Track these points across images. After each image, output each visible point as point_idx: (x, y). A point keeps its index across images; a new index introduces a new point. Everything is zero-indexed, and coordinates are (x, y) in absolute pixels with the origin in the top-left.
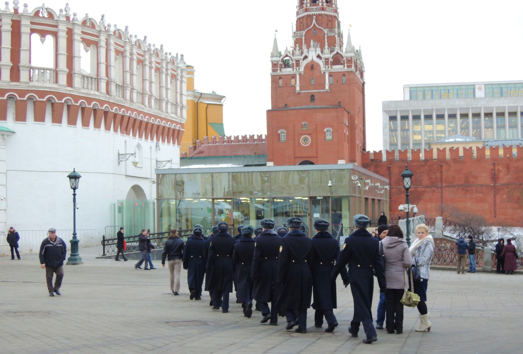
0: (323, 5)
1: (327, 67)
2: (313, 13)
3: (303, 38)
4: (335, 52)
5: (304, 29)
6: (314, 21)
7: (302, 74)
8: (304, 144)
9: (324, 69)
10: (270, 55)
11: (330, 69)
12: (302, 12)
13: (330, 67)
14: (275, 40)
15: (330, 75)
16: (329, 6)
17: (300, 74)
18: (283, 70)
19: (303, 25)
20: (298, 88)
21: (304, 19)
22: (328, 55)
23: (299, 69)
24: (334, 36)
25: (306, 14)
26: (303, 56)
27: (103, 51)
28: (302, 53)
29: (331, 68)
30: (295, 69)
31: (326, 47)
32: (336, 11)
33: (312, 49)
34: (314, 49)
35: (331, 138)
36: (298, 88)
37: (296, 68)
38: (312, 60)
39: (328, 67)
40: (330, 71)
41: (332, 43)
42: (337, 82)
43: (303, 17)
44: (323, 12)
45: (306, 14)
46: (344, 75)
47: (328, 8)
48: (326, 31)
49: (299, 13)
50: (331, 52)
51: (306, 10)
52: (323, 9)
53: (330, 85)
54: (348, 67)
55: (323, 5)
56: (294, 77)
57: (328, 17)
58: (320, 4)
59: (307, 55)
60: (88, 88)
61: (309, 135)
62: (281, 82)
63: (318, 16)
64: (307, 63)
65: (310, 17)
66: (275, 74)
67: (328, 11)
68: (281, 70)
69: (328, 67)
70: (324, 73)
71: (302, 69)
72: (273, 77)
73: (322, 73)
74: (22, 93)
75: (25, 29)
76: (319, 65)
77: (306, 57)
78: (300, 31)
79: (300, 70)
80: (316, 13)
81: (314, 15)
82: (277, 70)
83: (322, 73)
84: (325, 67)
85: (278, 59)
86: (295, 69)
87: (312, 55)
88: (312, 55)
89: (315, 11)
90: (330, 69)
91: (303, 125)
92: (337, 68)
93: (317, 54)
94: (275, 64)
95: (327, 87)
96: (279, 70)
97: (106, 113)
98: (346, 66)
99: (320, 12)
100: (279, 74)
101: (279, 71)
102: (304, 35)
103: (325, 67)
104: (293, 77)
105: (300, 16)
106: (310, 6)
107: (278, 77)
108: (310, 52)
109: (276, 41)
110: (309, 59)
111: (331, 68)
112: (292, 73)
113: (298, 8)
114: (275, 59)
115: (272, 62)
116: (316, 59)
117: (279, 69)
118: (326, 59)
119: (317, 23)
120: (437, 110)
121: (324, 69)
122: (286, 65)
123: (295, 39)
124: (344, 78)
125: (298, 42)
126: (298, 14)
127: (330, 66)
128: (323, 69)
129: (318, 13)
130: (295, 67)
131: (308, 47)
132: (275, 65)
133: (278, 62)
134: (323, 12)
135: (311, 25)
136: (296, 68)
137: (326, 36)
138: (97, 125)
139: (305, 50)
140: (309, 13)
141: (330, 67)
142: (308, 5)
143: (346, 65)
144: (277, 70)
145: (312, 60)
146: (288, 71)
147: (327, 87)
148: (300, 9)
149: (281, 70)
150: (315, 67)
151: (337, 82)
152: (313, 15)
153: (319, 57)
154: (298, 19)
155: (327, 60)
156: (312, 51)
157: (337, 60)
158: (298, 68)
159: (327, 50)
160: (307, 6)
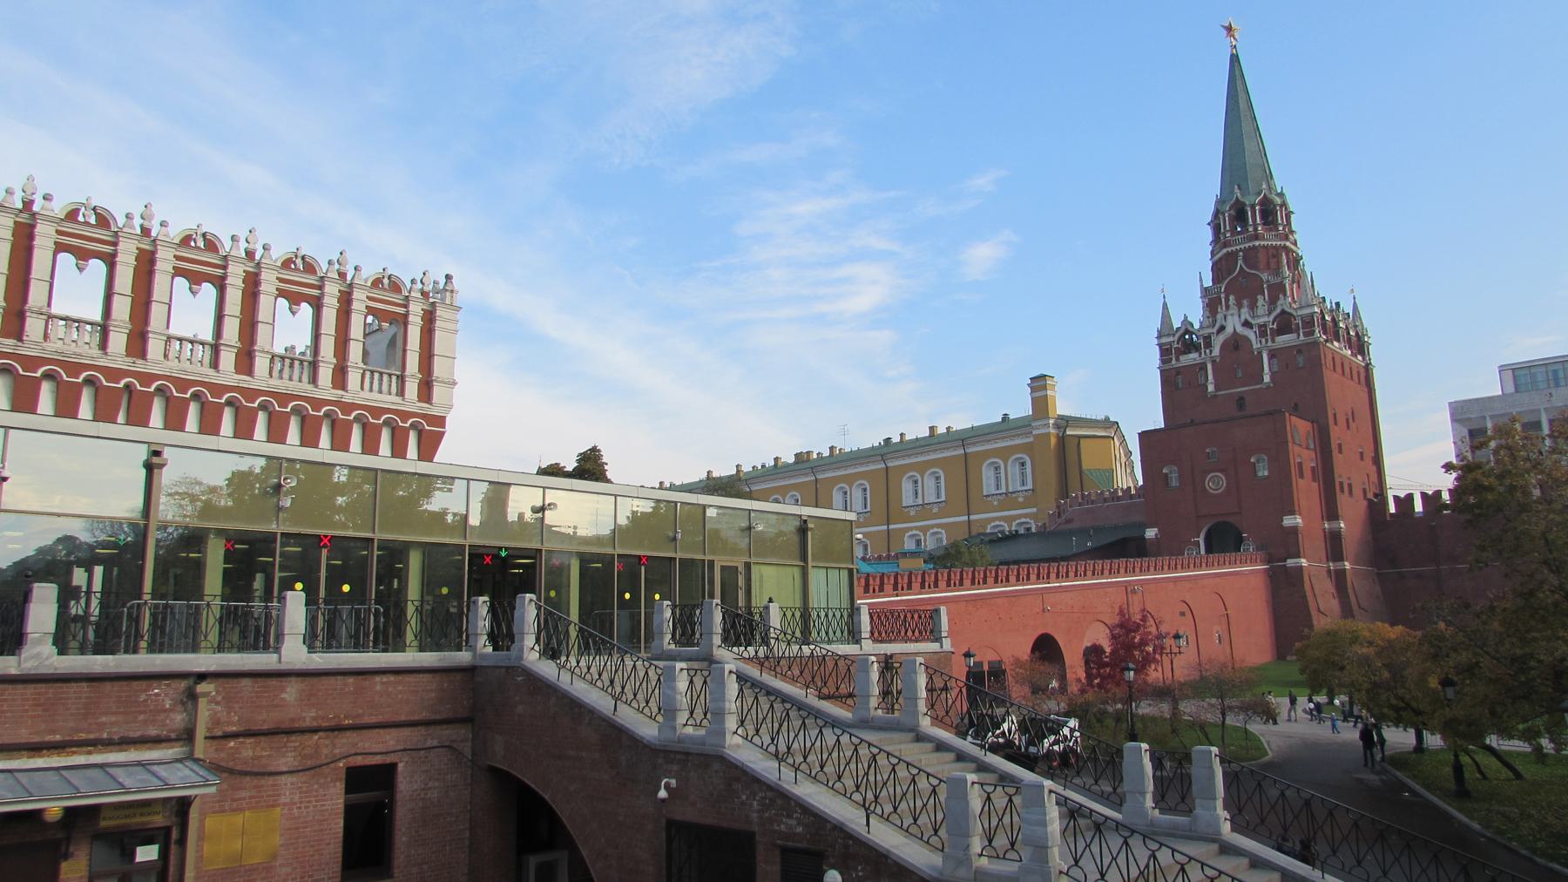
1: (1263, 340)
2: (1238, 248)
4: (1278, 311)
6: (1240, 262)
7: (1218, 360)
8: (1214, 490)
9: (1259, 345)
11: (1270, 344)
14: (1165, 306)
15: (1272, 356)
16: (1271, 230)
17: (1214, 362)
18: (1182, 358)
20: (1211, 388)
21: (1223, 262)
22: (1264, 317)
23: (1211, 352)
25: (1225, 251)
28: (1215, 322)
29: (1273, 341)
35: (1266, 473)
36: (1211, 388)
39: (1267, 341)
40: (1271, 348)
42: (1287, 368)
44: (1257, 243)
45: (1225, 251)
46: (1299, 352)
48: (1264, 276)
51: (1225, 245)
52: (1256, 237)
53: (1273, 375)
54: (1306, 334)
55: (1256, 229)
58: (1251, 229)
59: (1225, 324)
61: (1221, 471)
66: (1167, 367)
67: (1267, 240)
68: (1177, 360)
69: (1267, 341)
70: (1260, 353)
71: (1216, 352)
76: (1248, 340)
78: (1218, 283)
79: (1213, 355)
80: (1242, 247)
81: (1241, 250)
85: (1171, 339)
87: (1233, 324)
89: (1242, 243)
90: (1270, 344)
91: (1209, 453)
95: (1267, 379)
96: (1174, 359)
101: (1174, 362)
102: (1223, 290)
104: (1201, 369)
107: (1174, 373)
108: (1229, 318)
109: (1167, 308)
110: (1229, 330)
111: (1273, 341)
114: (1164, 340)
115: (1160, 345)
116: (1240, 329)
118: (1260, 326)
119: (1246, 266)
121: (1259, 345)
122: (1190, 346)
124: (1300, 360)
126: (1213, 254)
127: (1269, 337)
128: (1256, 346)
129: (1247, 245)
132: (1165, 352)
134: (1257, 243)
135: (1234, 271)
137: (1265, 286)
140: (1229, 249)
142: (1228, 235)
144: (1171, 359)
146: (1192, 358)
147: (1267, 379)
149: (1177, 360)
151: (1287, 368)
153: (1246, 324)
155: (1263, 328)
156: (1232, 315)
157: (1285, 324)
160: (1226, 237)
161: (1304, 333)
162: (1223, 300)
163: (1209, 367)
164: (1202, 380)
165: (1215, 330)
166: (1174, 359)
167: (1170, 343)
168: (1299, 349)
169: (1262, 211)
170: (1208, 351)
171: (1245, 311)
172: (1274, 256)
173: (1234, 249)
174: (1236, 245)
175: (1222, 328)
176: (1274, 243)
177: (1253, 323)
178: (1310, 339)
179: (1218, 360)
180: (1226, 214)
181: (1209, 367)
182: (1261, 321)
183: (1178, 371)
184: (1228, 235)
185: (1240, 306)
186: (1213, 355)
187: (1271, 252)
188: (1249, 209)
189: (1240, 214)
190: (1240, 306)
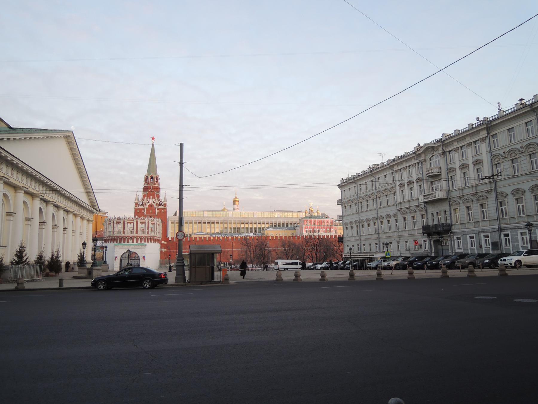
6: (151, 188)
10: (134, 200)
15: (158, 209)
16: (157, 183)
17: (146, 208)
20: (145, 213)
25: (148, 185)
26: (148, 201)
28: (147, 200)
31: (157, 199)
32: (159, 185)
33: (151, 199)
34: (152, 199)
36: (145, 213)
38: (151, 203)
41: (158, 196)
44: (155, 185)
45: (148, 185)
46: (163, 210)
47: (156, 184)
48: (156, 192)
50: (159, 201)
51: (149, 184)
52: (155, 184)
54: (165, 207)
56: (144, 209)
58: (154, 182)
62: (138, 211)
63: (152, 186)
65: (150, 186)
66: (136, 207)
71: (147, 206)
74: (149, 237)
75: (150, 223)
76: (153, 205)
77: (149, 202)
82: (137, 206)
87: (151, 201)
88: (151, 201)
92: (161, 207)
95: (156, 214)
97: (153, 239)
99: (154, 185)
105: (145, 186)
108: (150, 200)
110: (150, 203)
112: (143, 207)
114: (136, 202)
115: (135, 203)
118: (156, 203)
120: (190, 221)
123: (143, 194)
124: (163, 211)
125: (144, 196)
126: (144, 184)
131: (150, 199)
134: (155, 185)
138: (154, 242)
139: (149, 199)
142: (149, 182)
145: (151, 203)
147: (156, 214)
150: (152, 206)
153: (154, 202)
154: (144, 187)
155: (157, 204)
159: (157, 200)
163: (145, 209)
164: (143, 212)
167: (137, 203)
171: (154, 200)
178: (165, 208)
181: (145, 209)
183: (138, 209)
184: (149, 182)
185: (153, 199)
189: (152, 178)
190: (153, 199)
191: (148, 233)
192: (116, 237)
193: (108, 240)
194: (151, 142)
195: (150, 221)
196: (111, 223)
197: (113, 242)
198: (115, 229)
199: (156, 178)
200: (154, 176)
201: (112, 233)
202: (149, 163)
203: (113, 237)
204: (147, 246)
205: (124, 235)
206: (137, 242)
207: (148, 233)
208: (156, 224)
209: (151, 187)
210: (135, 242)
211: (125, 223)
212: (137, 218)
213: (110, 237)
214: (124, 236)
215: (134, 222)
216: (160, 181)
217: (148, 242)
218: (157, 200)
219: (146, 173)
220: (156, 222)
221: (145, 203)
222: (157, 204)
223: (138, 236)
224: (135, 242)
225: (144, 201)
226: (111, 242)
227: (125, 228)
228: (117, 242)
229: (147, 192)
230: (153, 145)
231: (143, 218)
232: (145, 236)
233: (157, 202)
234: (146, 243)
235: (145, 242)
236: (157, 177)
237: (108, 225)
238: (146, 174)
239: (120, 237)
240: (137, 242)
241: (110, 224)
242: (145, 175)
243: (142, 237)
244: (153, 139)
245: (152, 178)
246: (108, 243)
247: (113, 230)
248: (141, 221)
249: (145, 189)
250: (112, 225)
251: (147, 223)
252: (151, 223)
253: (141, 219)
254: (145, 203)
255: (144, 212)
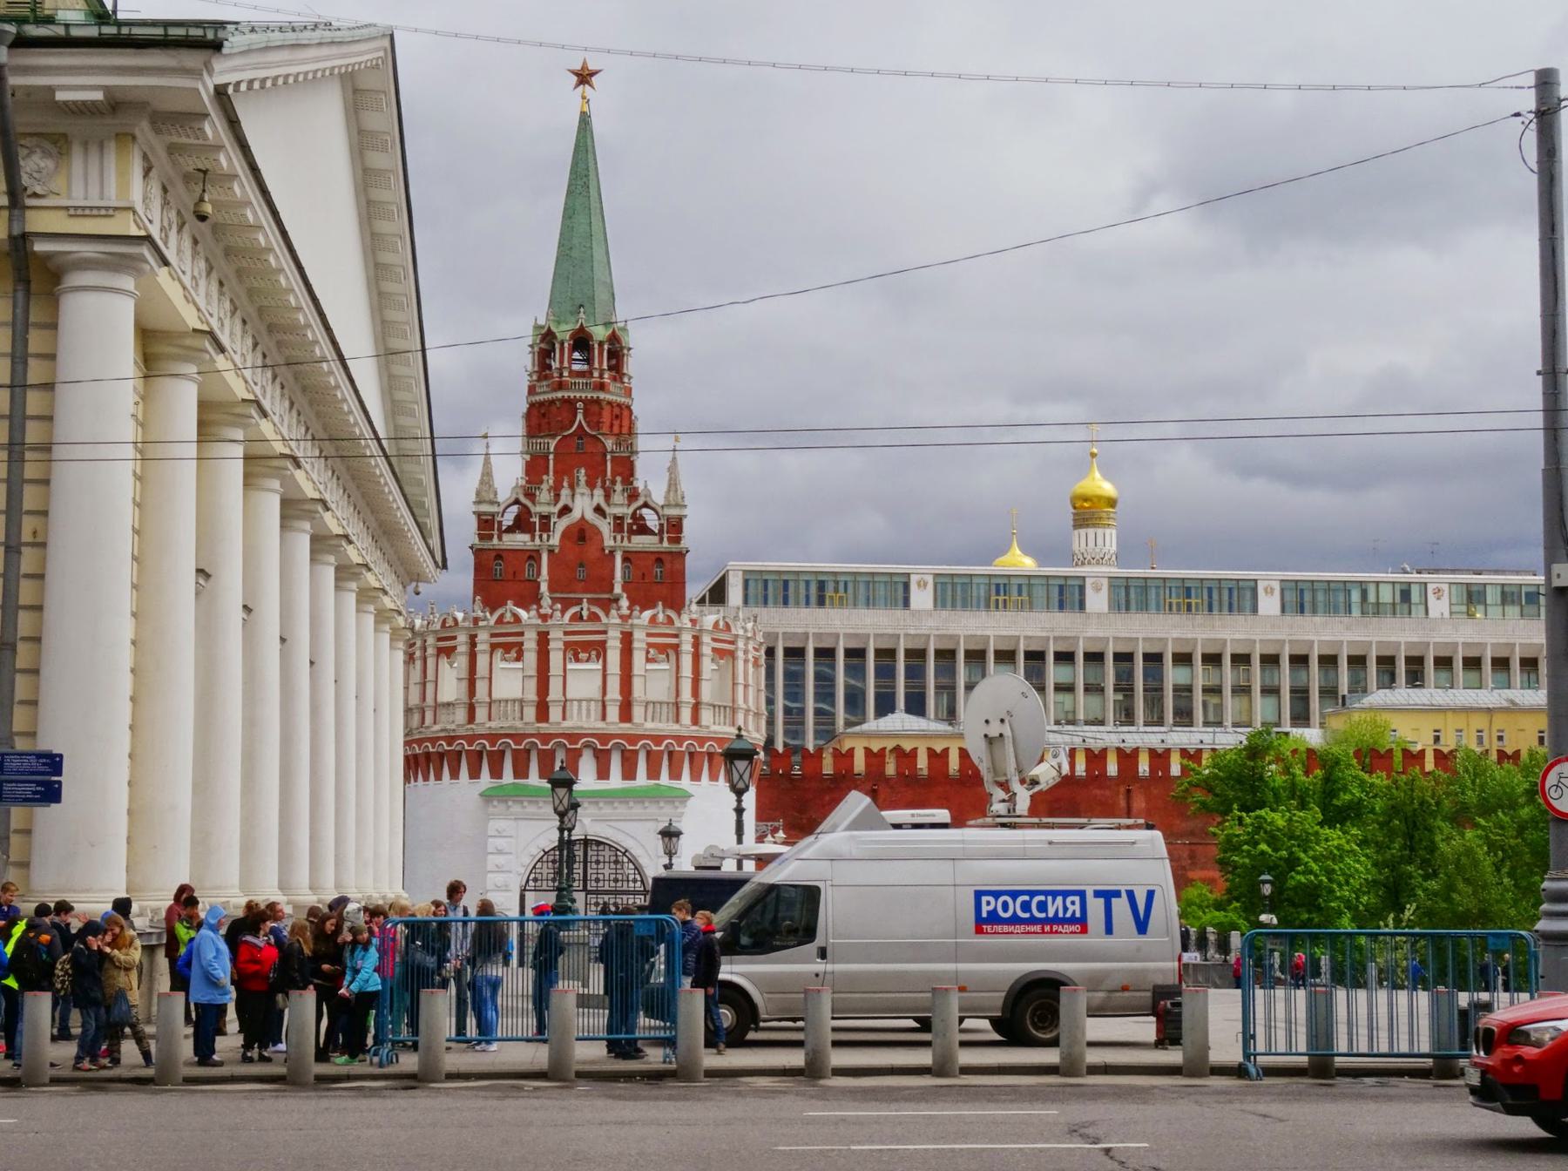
0: (601, 376)
1: (619, 537)
2: (578, 395)
3: (551, 457)
4: (640, 502)
5: (553, 436)
6: (580, 417)
9: (612, 543)
10: (473, 498)
11: (625, 543)
12: (545, 389)
13: (626, 539)
15: (625, 559)
17: (551, 552)
18: (506, 537)
19: (549, 423)
21: (553, 408)
23: (549, 536)
24: (629, 457)
25: (559, 395)
26: (560, 505)
27: (740, 665)
28: (557, 497)
29: (629, 541)
30: (537, 538)
33: (582, 488)
34: (587, 491)
37: (541, 536)
38: (583, 518)
43: (552, 402)
44: (602, 395)
45: (559, 395)
48: (609, 443)
49: (538, 390)
51: (561, 386)
52: (601, 387)
54: (671, 540)
55: (601, 376)
56: (534, 556)
57: (612, 407)
58: (596, 374)
59: (570, 505)
60: (719, 724)
63: (586, 401)
64: (568, 523)
65: (570, 403)
66: (486, 545)
70: (612, 553)
71: (555, 540)
72: (478, 552)
73: (607, 552)
75: (706, 650)
76: (599, 533)
80: (583, 395)
82: (491, 537)
83: (607, 552)
84: (615, 538)
86: (537, 538)
87: (583, 505)
88: (583, 505)
89: (579, 390)
90: (625, 543)
92: (641, 542)
93: (595, 504)
94: (487, 521)
96: (496, 537)
98: (665, 539)
100: (497, 547)
101: (495, 541)
102: (552, 450)
103: (615, 538)
104: (530, 558)
106: (569, 376)
107: (493, 554)
108: (578, 498)
110: (576, 515)
111: (629, 541)
112: (530, 545)
113: (535, 377)
115: (479, 515)
116: (591, 516)
117: (495, 532)
118: (616, 518)
120: (818, 636)
121: (612, 543)
125: (535, 468)
126: (532, 390)
127: (625, 534)
128: (609, 542)
129: (589, 396)
130: (537, 533)
131: (572, 487)
133: (493, 516)
134: (602, 395)
135: (571, 427)
136: (541, 536)
137: (609, 457)
139: (565, 492)
140: (567, 395)
141: (626, 539)
143: (665, 535)
144: (493, 535)
145: (583, 518)
146: (520, 540)
148: (539, 380)
149: (500, 538)
151: (643, 579)
152: (576, 400)
153: (598, 510)
154: (532, 405)
155: (618, 520)
158: (545, 536)
159: (619, 497)
160: (561, 375)
161: (669, 538)
162: (551, 462)
165: (556, 510)
166: (496, 537)
167: (493, 515)
168: (659, 558)
169: (609, 351)
170: (545, 536)
171: (599, 492)
172: (617, 417)
173: (572, 395)
174: (575, 390)
175: (566, 510)
176: (619, 399)
177: (608, 510)
178: (674, 548)
179: (557, 551)
180: (566, 345)
182: (618, 511)
183: (499, 555)
184: (566, 374)
185: (591, 485)
186: (551, 542)
187: (617, 411)
188: (596, 346)
191: (696, 720)
192: (493, 737)
193: (422, 760)
194: (570, 102)
195: (706, 639)
196: (454, 648)
197: (475, 774)
198: (481, 687)
199: (606, 347)
200: (599, 333)
201: (461, 715)
202: (561, 245)
203: (471, 739)
204: (691, 802)
205: (544, 727)
206: (629, 773)
207: (696, 720)
208: (740, 654)
209: (580, 405)
210: (616, 781)
211: (552, 645)
212: (625, 611)
213: (451, 740)
214: (546, 738)
215: (609, 644)
216: (631, 366)
217: (696, 776)
218: (619, 497)
219: (540, 313)
220: (741, 644)
221: (545, 519)
222: (618, 520)
223: (633, 739)
224: (616, 781)
225: (534, 502)
226: (455, 774)
227: (552, 680)
228: (496, 773)
229: (553, 444)
230: (585, 120)
231: (661, 617)
232: (680, 739)
233: (620, 506)
234: (685, 782)
235: (675, 774)
236: (614, 338)
237: (431, 662)
238: (542, 322)
239: (517, 737)
240: (629, 773)
241: (448, 652)
242: (537, 327)
243: (658, 739)
244: (584, 77)
245: (582, 341)
246: (438, 777)
247: (604, 693)
248: (649, 635)
249: (540, 419)
250: (461, 661)
251: (687, 647)
252: (714, 650)
253: (653, 619)
254: (545, 519)
255: (539, 573)
